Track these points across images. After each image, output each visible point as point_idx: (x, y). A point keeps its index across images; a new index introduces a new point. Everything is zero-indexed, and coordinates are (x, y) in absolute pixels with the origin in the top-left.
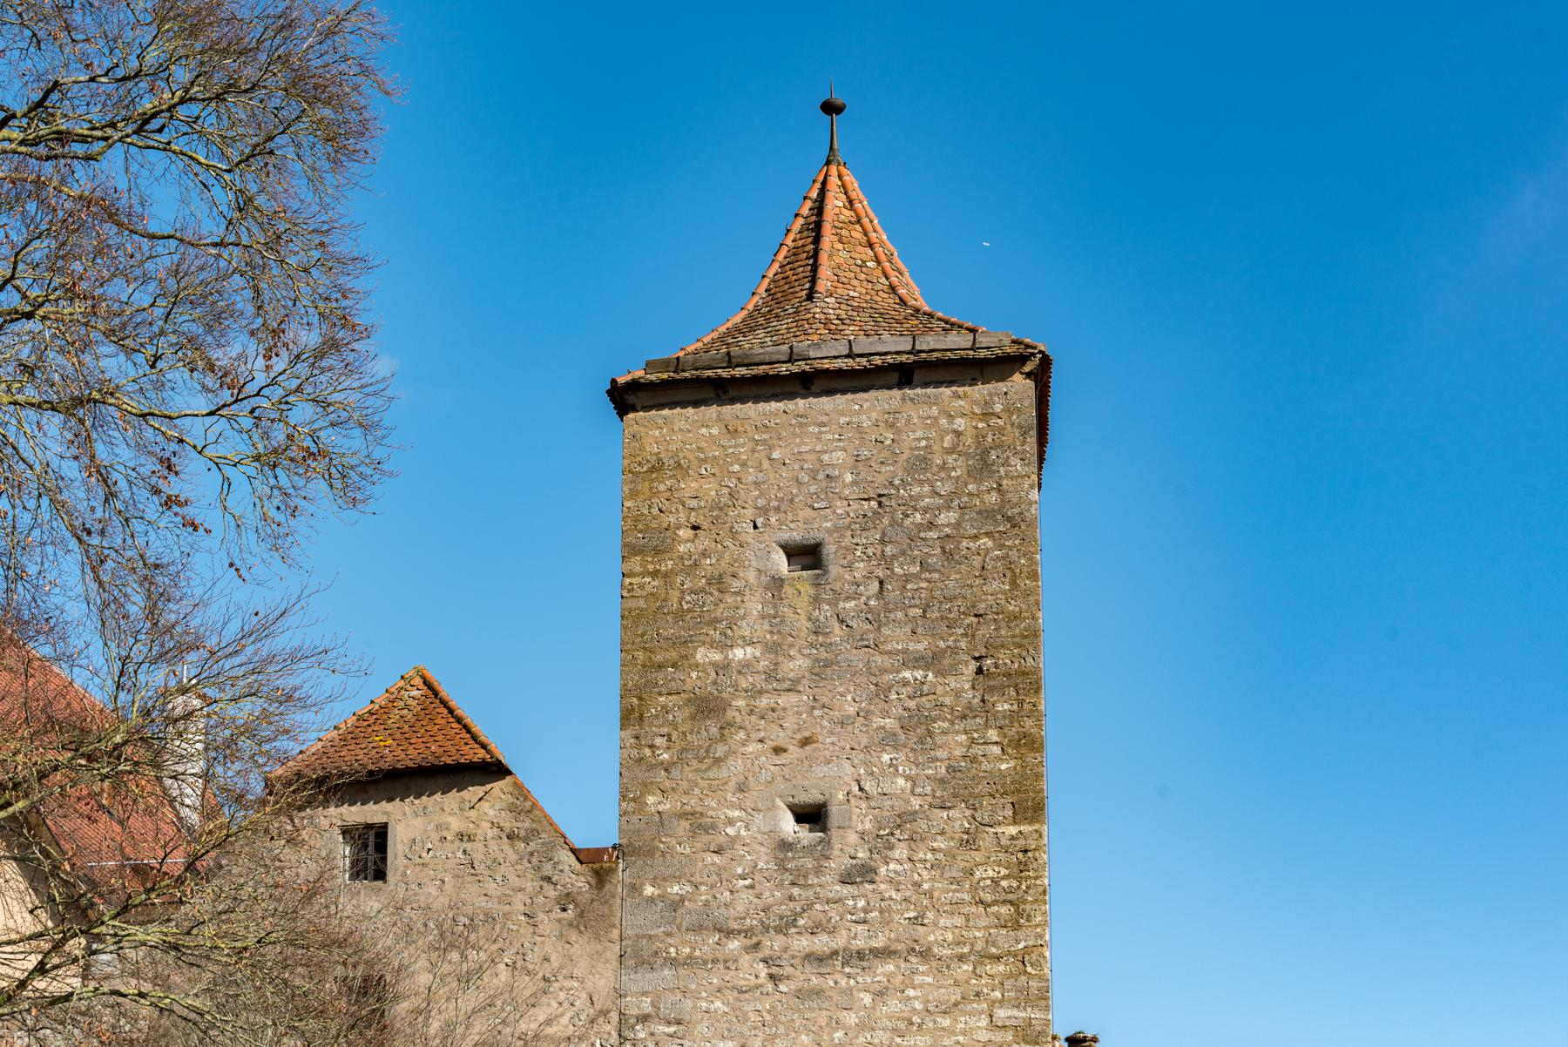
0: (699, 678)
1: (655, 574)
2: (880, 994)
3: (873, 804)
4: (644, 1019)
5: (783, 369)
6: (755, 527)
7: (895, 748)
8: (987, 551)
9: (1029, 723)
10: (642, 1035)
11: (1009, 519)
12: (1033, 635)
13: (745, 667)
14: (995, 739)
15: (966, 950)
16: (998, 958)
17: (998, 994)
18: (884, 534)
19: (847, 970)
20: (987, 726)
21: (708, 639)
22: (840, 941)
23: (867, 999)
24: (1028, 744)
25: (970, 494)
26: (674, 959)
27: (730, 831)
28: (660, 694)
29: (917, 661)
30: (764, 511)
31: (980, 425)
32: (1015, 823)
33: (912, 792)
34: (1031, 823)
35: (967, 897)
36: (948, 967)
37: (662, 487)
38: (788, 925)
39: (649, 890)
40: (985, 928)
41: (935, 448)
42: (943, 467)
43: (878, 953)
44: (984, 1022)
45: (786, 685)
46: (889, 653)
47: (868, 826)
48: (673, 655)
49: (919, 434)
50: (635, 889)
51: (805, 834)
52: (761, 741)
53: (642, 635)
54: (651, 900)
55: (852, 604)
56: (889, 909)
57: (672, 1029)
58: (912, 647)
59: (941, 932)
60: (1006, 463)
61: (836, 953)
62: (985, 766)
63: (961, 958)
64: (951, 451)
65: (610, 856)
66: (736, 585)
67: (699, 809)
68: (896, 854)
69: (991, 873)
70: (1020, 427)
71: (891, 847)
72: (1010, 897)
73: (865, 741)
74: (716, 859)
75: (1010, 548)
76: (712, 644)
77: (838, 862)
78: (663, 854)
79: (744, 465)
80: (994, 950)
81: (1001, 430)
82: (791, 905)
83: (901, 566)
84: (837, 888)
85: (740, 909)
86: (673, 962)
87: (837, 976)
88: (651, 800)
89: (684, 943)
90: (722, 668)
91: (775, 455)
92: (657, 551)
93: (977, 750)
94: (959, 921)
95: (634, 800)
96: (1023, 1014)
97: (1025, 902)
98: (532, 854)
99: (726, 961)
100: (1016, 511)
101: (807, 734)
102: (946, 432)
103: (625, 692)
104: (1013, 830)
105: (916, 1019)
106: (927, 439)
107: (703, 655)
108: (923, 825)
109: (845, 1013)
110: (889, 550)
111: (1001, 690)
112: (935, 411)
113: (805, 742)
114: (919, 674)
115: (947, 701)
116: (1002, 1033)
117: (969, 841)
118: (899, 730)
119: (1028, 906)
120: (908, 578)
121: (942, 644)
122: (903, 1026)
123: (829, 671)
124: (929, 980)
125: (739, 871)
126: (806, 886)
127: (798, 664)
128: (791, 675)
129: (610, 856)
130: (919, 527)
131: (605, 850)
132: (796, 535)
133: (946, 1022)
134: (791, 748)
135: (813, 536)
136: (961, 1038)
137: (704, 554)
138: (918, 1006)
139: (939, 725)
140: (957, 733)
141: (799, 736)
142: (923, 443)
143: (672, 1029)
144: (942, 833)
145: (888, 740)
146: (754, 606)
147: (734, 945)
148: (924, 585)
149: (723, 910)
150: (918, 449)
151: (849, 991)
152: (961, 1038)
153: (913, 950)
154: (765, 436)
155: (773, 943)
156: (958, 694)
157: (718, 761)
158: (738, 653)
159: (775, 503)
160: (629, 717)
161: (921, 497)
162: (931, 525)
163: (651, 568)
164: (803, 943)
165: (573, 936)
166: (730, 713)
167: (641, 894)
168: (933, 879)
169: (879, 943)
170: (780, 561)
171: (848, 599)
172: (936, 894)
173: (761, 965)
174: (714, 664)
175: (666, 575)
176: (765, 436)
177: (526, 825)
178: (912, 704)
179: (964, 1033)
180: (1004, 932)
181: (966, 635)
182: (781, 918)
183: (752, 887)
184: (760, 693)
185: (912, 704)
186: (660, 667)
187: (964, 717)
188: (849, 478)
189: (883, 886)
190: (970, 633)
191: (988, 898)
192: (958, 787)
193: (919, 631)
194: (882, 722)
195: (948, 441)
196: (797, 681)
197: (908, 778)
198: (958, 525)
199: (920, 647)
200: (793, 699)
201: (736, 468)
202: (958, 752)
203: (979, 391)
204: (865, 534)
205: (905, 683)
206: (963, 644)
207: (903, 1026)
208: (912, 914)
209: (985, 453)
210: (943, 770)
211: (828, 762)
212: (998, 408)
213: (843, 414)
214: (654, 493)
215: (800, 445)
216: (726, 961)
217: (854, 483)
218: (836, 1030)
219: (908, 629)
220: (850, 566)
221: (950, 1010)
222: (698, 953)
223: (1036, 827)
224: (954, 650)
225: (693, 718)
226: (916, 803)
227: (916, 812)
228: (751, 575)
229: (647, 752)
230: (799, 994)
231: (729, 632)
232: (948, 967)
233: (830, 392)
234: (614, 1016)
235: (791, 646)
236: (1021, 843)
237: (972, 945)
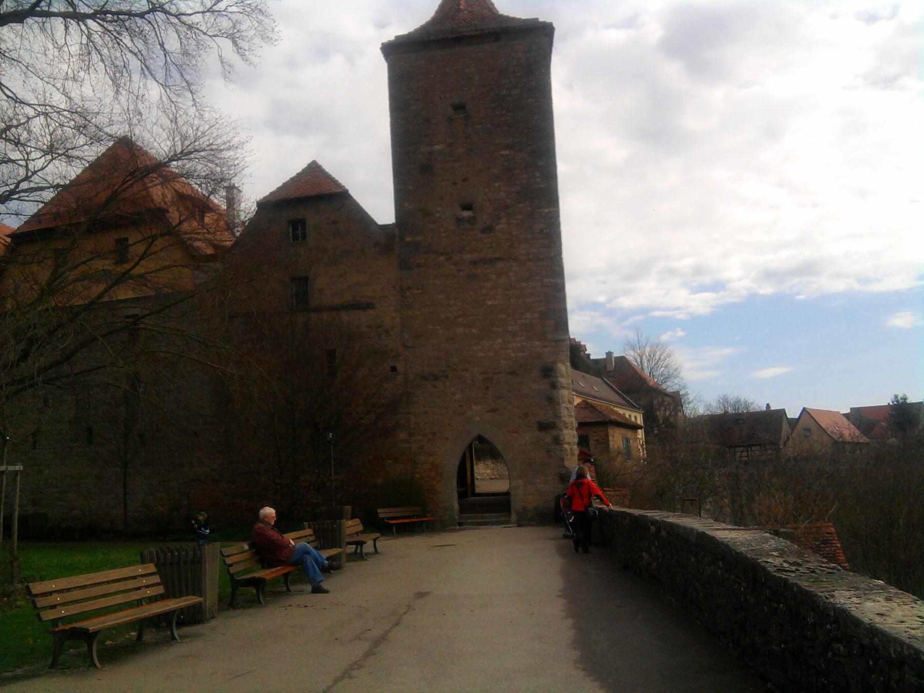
4: (409, 288)
23: (494, 277)
27: (438, 215)
29: (507, 147)
39: (408, 239)
51: (467, 214)
63: (530, 260)
113: (465, 180)
114: (507, 152)
147: (442, 258)
158: (438, 147)
169: (497, 255)
170: (450, 110)
205: (502, 155)
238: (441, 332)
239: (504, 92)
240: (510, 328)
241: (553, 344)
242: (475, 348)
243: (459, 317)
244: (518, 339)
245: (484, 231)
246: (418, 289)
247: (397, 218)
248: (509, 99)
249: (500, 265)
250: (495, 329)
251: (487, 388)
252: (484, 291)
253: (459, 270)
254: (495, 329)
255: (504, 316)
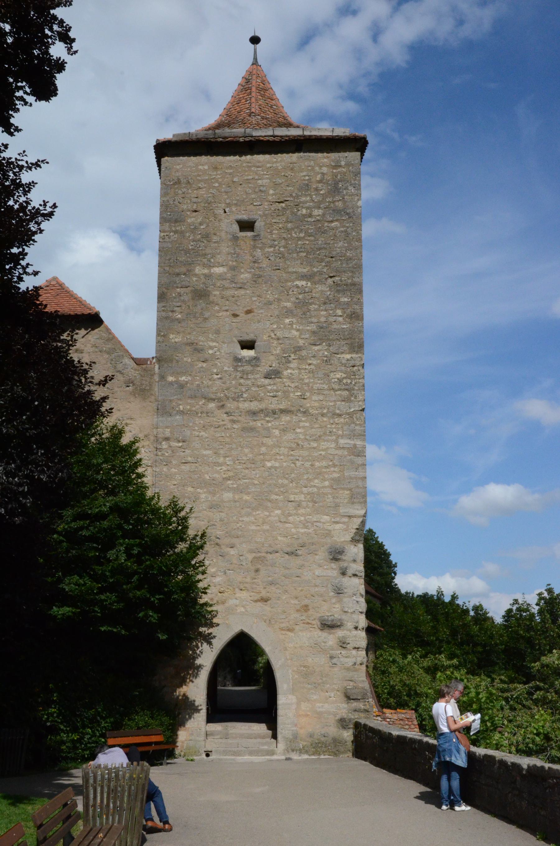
0: (196, 281)
1: (176, 232)
2: (284, 431)
3: (280, 342)
4: (167, 439)
5: (241, 140)
6: (225, 212)
7: (294, 316)
8: (337, 228)
9: (356, 307)
10: (164, 447)
11: (347, 214)
12: (358, 268)
13: (221, 277)
14: (340, 314)
15: (325, 411)
16: (340, 415)
17: (340, 432)
18: (288, 218)
19: (267, 419)
20: (336, 308)
21: (201, 263)
22: (262, 406)
23: (277, 432)
24: (356, 316)
25: (329, 202)
26: (182, 411)
27: (211, 352)
28: (177, 287)
29: (303, 277)
30: (229, 205)
31: (334, 171)
32: (349, 353)
33: (299, 337)
34: (357, 353)
35: (326, 387)
36: (317, 419)
37: (180, 192)
38: (238, 397)
39: (170, 379)
40: (335, 401)
41: (313, 180)
42: (317, 189)
43: (282, 411)
44: (333, 445)
45: (238, 286)
46: (289, 272)
47: (278, 352)
48: (183, 269)
49: (305, 173)
50: (162, 377)
51: (248, 353)
52: (227, 311)
53: (169, 260)
54: (171, 383)
55: (272, 249)
56: (288, 391)
57: (180, 444)
58: (300, 270)
59: (313, 402)
60: (346, 189)
61: (262, 410)
62: (335, 326)
63: (323, 415)
64: (320, 182)
65: (151, 362)
66: (215, 238)
67: (196, 341)
68: (292, 365)
69: (338, 376)
70: (353, 172)
71: (290, 362)
72: (347, 387)
73: (277, 313)
74: (204, 365)
75: (348, 227)
76: (204, 266)
77: (264, 368)
78: (177, 361)
79: (220, 184)
80: (338, 412)
81: (345, 173)
82: (240, 387)
83: (295, 233)
84: (263, 380)
85: (215, 389)
86: (182, 413)
87: (262, 422)
88: (171, 336)
89: (188, 404)
90: (208, 276)
91: (235, 179)
92: (176, 221)
93: (332, 319)
94: (321, 397)
95: (164, 336)
96: (352, 442)
97: (354, 389)
98: (112, 360)
99: (207, 413)
100: (351, 210)
101: (249, 308)
102: (318, 173)
103: (160, 286)
104: (348, 356)
105: (300, 442)
106: (309, 176)
107: (198, 270)
108: (304, 353)
109: (265, 439)
110: (289, 225)
111: (344, 291)
112: (312, 163)
113: (249, 312)
114: (304, 283)
115: (317, 295)
116: (342, 451)
117: (327, 361)
118: (294, 308)
119: (355, 392)
120: (299, 239)
121: (315, 270)
122: (294, 446)
123: (260, 280)
124: (307, 424)
125: (215, 371)
126: (247, 379)
127: (245, 276)
128: (241, 281)
129: (151, 362)
130: (304, 216)
131: (148, 359)
132: (244, 217)
133: (315, 445)
134: (241, 315)
135: (252, 217)
136: (323, 453)
137: (201, 224)
138: (302, 437)
139: (312, 307)
140: (322, 310)
141: (245, 309)
142: (307, 178)
143: (180, 444)
144: (314, 357)
145: (289, 313)
146: (225, 248)
147: (212, 405)
148: (307, 242)
149: (207, 389)
150: (304, 180)
151: (268, 429)
152: (323, 453)
153: (299, 410)
154: (231, 171)
155: (231, 405)
156: (322, 291)
157: (206, 319)
159: (235, 202)
160: (162, 297)
161: (306, 202)
162: (310, 216)
163: (173, 229)
164: (245, 406)
165: (132, 399)
166: (211, 298)
167: (166, 380)
168: (309, 378)
169: (282, 407)
171: (271, 247)
172: (311, 385)
173: (225, 415)
174: (205, 276)
175: (182, 232)
176: (231, 171)
177: (109, 346)
178: (300, 297)
179: (323, 450)
180: (343, 403)
181: (327, 266)
182: (235, 393)
183: (221, 378)
184: (227, 289)
185: (300, 297)
186: (178, 274)
187: (325, 303)
188: (271, 192)
189: (285, 380)
190: (328, 265)
191: (336, 387)
192: (322, 335)
193: (305, 263)
194: (285, 304)
195: (319, 177)
196: (245, 284)
197: (298, 330)
198: (324, 215)
199: (305, 270)
200: (242, 292)
201: (217, 185)
202: (323, 319)
203: (334, 156)
204: (278, 218)
205: (298, 287)
206: (325, 270)
207: (294, 446)
208: (299, 394)
209: (336, 184)
210: (315, 327)
211: (259, 322)
212: (343, 163)
213: (269, 163)
214: (176, 194)
215: (248, 175)
216: (207, 413)
217: (273, 195)
218: (260, 447)
219: (299, 262)
220: (271, 233)
221: (318, 439)
222: (194, 409)
223: (360, 355)
224: (321, 273)
225: (193, 299)
226: (301, 342)
227: (301, 347)
228: (223, 234)
229: (170, 314)
230: (243, 429)
231: (212, 260)
232: (317, 419)
233: (264, 153)
234: (152, 438)
235: (242, 267)
236: (352, 363)
237: (328, 409)
238: (203, 496)
239: (304, 211)
240: (292, 497)
241: (346, 520)
242: (245, 519)
243: (228, 479)
244: (302, 511)
245: (267, 376)
246: (179, 441)
247: (157, 351)
248: (309, 219)
249: (285, 418)
250: (274, 497)
251: (257, 571)
252: (263, 449)
253: (234, 422)
254: (274, 497)
255: (286, 482)
